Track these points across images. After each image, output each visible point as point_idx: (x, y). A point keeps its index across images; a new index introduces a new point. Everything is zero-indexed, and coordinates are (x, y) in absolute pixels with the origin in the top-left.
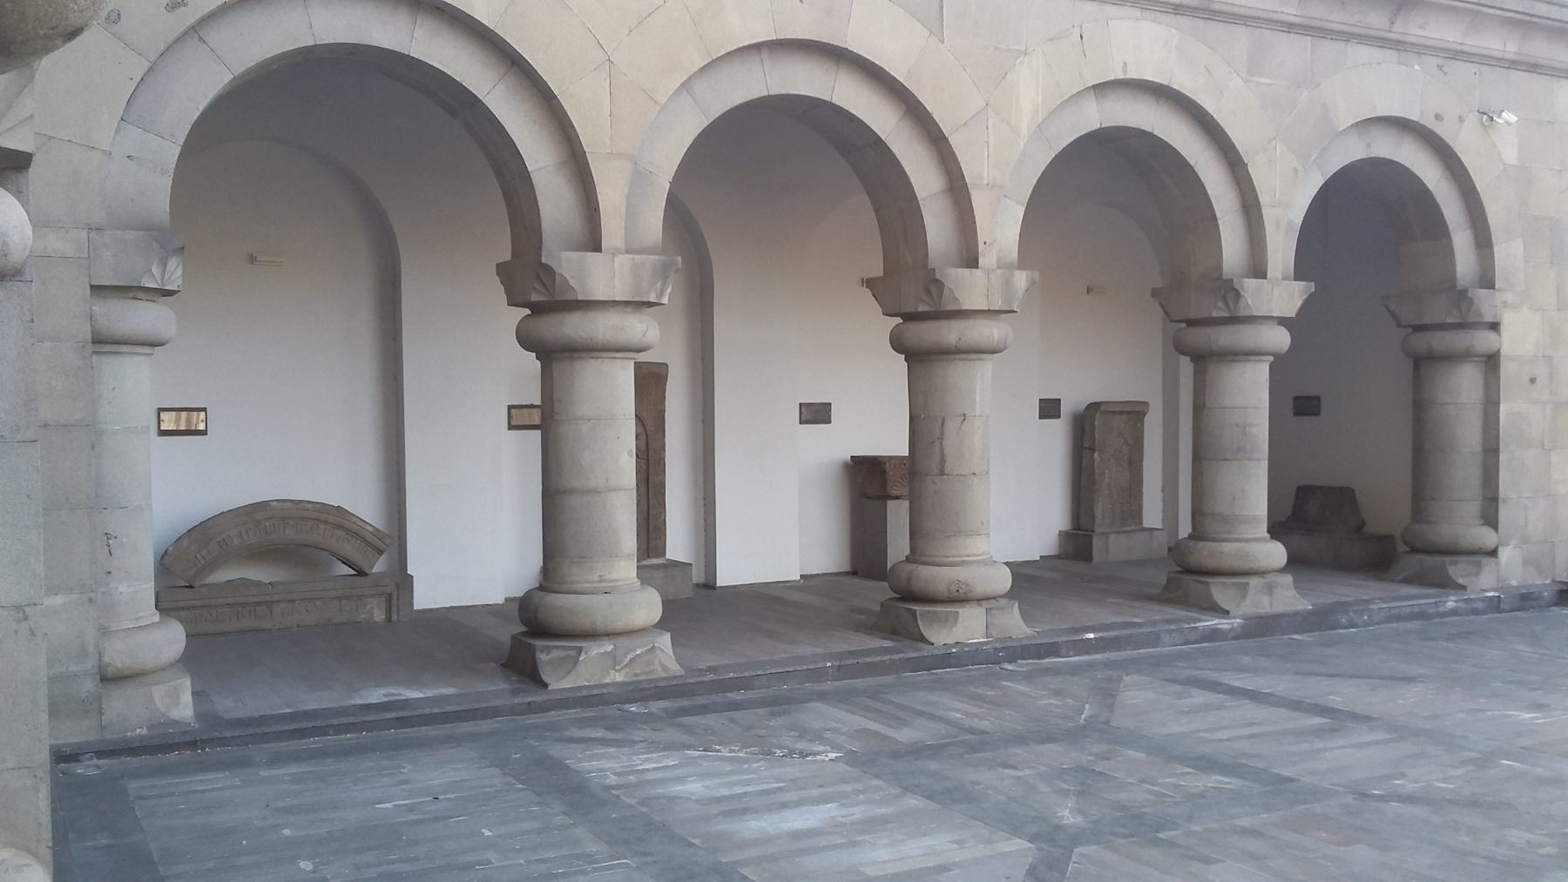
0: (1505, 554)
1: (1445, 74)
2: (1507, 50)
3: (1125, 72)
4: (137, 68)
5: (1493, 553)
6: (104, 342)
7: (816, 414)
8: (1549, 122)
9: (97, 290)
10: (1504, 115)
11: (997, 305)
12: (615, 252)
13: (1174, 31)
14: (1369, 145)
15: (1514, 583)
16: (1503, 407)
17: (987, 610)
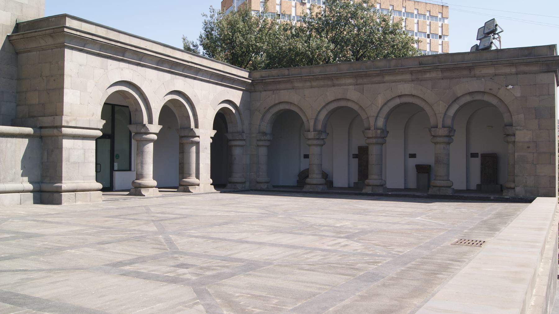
0: (517, 189)
3: (401, 93)
4: (261, 116)
5: (514, 188)
7: (413, 156)
10: (509, 86)
11: (374, 136)
12: (312, 132)
15: (521, 196)
16: (515, 154)
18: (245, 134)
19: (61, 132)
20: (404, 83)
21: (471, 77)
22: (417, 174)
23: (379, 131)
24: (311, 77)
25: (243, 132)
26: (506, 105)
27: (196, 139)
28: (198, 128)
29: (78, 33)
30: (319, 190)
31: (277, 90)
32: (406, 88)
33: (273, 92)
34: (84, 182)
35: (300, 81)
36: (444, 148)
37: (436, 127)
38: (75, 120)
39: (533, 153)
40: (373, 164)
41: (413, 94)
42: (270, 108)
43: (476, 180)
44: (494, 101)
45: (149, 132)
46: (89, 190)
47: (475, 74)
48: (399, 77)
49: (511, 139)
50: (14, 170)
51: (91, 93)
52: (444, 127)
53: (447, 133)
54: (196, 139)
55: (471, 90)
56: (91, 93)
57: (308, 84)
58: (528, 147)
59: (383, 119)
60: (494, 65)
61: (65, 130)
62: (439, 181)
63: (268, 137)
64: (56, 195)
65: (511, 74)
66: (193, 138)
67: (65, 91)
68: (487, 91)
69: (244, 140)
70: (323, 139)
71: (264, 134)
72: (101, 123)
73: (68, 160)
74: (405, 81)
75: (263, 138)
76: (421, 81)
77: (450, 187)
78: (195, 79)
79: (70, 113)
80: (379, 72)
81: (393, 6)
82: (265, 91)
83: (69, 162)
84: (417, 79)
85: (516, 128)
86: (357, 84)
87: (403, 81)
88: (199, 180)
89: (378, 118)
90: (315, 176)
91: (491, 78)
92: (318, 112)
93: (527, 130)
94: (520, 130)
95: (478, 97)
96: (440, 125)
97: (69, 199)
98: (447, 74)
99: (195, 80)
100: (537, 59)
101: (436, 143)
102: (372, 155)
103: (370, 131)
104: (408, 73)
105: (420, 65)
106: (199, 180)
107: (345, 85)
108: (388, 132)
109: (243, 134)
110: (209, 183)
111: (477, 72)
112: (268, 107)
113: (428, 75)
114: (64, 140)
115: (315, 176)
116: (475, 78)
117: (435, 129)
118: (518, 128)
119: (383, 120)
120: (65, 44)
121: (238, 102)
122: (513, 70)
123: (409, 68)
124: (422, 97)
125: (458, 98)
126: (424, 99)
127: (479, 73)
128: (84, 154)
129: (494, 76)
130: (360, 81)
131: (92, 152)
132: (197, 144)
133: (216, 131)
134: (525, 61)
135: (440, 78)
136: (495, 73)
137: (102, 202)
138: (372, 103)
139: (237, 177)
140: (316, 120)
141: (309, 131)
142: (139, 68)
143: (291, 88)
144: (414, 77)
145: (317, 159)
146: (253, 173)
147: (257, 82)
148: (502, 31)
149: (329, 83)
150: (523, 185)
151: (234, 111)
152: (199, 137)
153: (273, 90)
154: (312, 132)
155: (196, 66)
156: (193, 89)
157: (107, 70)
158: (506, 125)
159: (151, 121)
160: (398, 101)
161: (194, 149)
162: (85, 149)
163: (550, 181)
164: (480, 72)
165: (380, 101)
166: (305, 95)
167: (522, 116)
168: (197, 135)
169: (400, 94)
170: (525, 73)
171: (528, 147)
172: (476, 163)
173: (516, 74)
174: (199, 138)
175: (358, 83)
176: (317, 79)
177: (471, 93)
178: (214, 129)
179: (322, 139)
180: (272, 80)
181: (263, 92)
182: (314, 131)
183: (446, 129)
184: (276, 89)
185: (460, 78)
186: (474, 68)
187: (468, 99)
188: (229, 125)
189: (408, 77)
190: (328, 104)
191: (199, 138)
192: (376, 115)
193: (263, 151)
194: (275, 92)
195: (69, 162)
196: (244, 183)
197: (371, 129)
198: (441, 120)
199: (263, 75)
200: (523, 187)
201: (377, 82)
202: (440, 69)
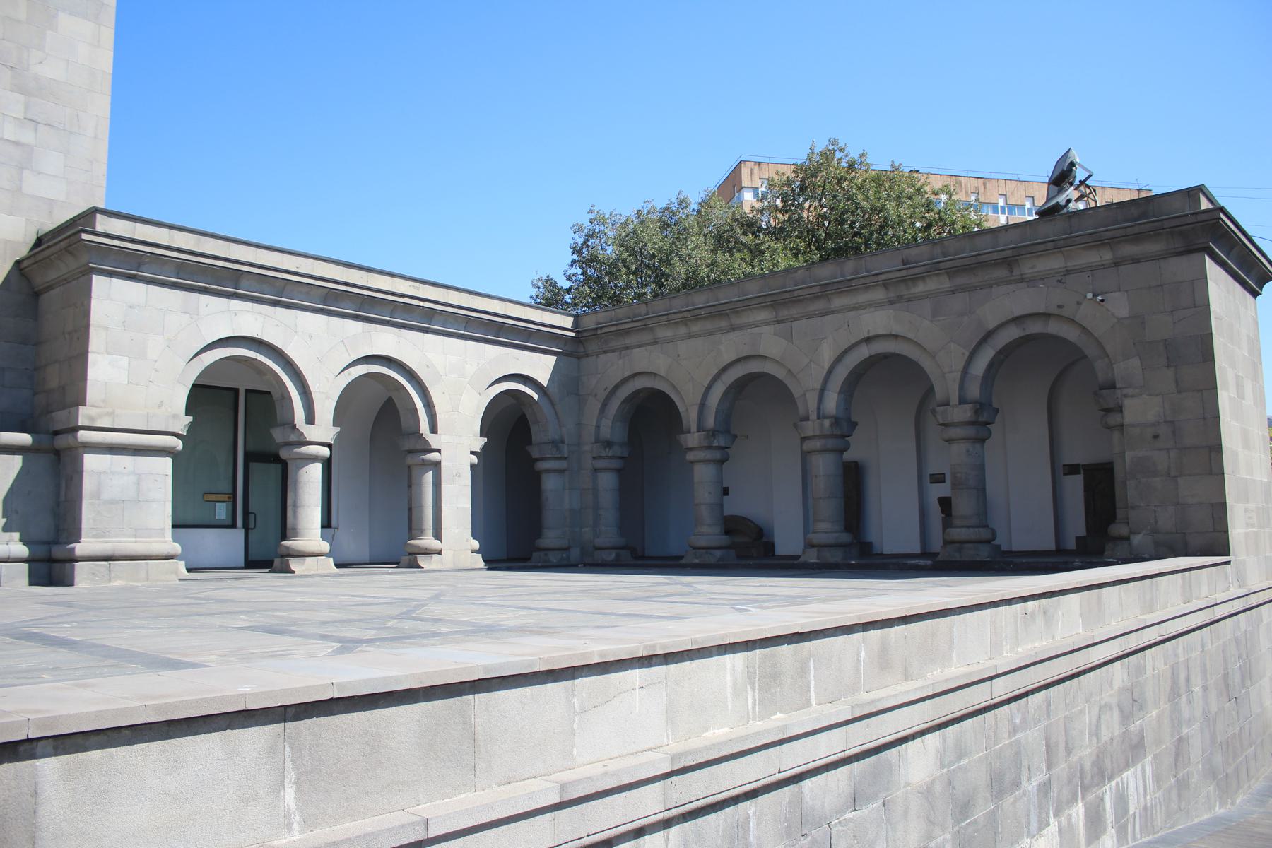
1: (1063, 283)
2: (1103, 259)
4: (599, 405)
5: (1128, 538)
6: (596, 470)
7: (938, 479)
8: (1158, 286)
9: (594, 458)
11: (818, 433)
12: (694, 433)
13: (891, 311)
14: (1024, 329)
17: (818, 551)
18: (566, 447)
19: (76, 438)
20: (873, 309)
21: (1016, 282)
22: (943, 517)
23: (827, 423)
24: (686, 314)
25: (563, 442)
26: (1097, 340)
27: (433, 456)
28: (437, 433)
29: (117, 243)
30: (713, 560)
31: (627, 348)
32: (877, 321)
33: (620, 354)
34: (136, 542)
35: (665, 324)
36: (968, 451)
37: (946, 404)
38: (111, 414)
39: (1168, 449)
40: (820, 498)
41: (893, 333)
42: (617, 387)
43: (1077, 525)
44: (1071, 334)
46: (146, 556)
47: (1022, 275)
48: (862, 298)
49: (1114, 419)
51: (156, 361)
52: (962, 401)
53: (969, 414)
54: (433, 456)
55: (1018, 313)
56: (156, 361)
57: (682, 330)
58: (1156, 437)
59: (836, 395)
60: (1059, 250)
61: (83, 436)
62: (958, 530)
63: (617, 451)
64: (68, 565)
65: (1103, 267)
67: (91, 357)
68: (1056, 311)
69: (565, 458)
70: (723, 448)
71: (608, 444)
72: (182, 423)
73: (97, 495)
74: (875, 305)
75: (603, 453)
76: (909, 300)
77: (988, 542)
78: (426, 331)
79: (104, 401)
80: (817, 289)
81: (1033, 197)
82: (605, 352)
84: (900, 298)
85: (1125, 391)
86: (778, 322)
87: (870, 305)
88: (441, 541)
89: (826, 393)
90: (704, 529)
91: (1059, 281)
92: (704, 388)
93: (1151, 395)
94: (1133, 396)
95: (1035, 328)
96: (954, 399)
97: (93, 574)
98: (961, 280)
99: (426, 334)
100: (1156, 224)
101: (950, 441)
102: (816, 476)
103: (810, 422)
104: (876, 285)
105: (904, 265)
106: (441, 541)
107: (755, 325)
108: (855, 425)
109: (561, 445)
110: (469, 547)
111: (1030, 267)
112: (610, 387)
113: (921, 288)
114: (86, 456)
115: (704, 529)
116: (1024, 284)
117: (945, 407)
118: (1130, 391)
119: (835, 395)
120: (90, 265)
121: (544, 378)
122: (1107, 256)
123: (877, 274)
124: (910, 335)
125: (988, 335)
126: (916, 342)
127: (1031, 271)
128: (138, 484)
129: (1065, 275)
130: (784, 313)
131: (157, 481)
132: (437, 465)
133: (486, 439)
134: (1129, 231)
135: (948, 291)
136: (1066, 267)
137: (177, 582)
138: (811, 361)
139: (551, 537)
140: (702, 406)
141: (689, 432)
142: (280, 310)
143: (652, 341)
144: (892, 294)
145: (710, 493)
146: (587, 529)
147: (585, 334)
148: (1090, 176)
149: (723, 323)
150: (1149, 527)
152: (439, 451)
153: (620, 350)
154: (694, 433)
155: (421, 304)
156: (422, 351)
157: (198, 315)
158: (1102, 388)
159: (310, 419)
160: (864, 352)
161: (429, 477)
162: (140, 475)
163: (1213, 515)
164: (1032, 268)
165: (827, 355)
166: (679, 356)
167: (1135, 362)
168: (434, 446)
169: (867, 335)
170: (1135, 260)
171: (1156, 437)
172: (1075, 487)
173: (1115, 266)
174: (440, 452)
175: (780, 319)
176: (698, 318)
177: (1018, 320)
178: (482, 435)
179: (716, 447)
180: (614, 328)
181: (602, 356)
182: (698, 431)
183: (968, 407)
184: (624, 346)
185: (992, 287)
186: (1017, 260)
187: (1013, 333)
188: (534, 429)
189: (879, 295)
190: (725, 369)
191: (440, 452)
192: (818, 386)
193: (607, 481)
194: (623, 352)
196: (566, 549)
197: (810, 418)
198: (957, 386)
199: (601, 321)
200: (1147, 534)
201: (817, 312)
202: (943, 271)
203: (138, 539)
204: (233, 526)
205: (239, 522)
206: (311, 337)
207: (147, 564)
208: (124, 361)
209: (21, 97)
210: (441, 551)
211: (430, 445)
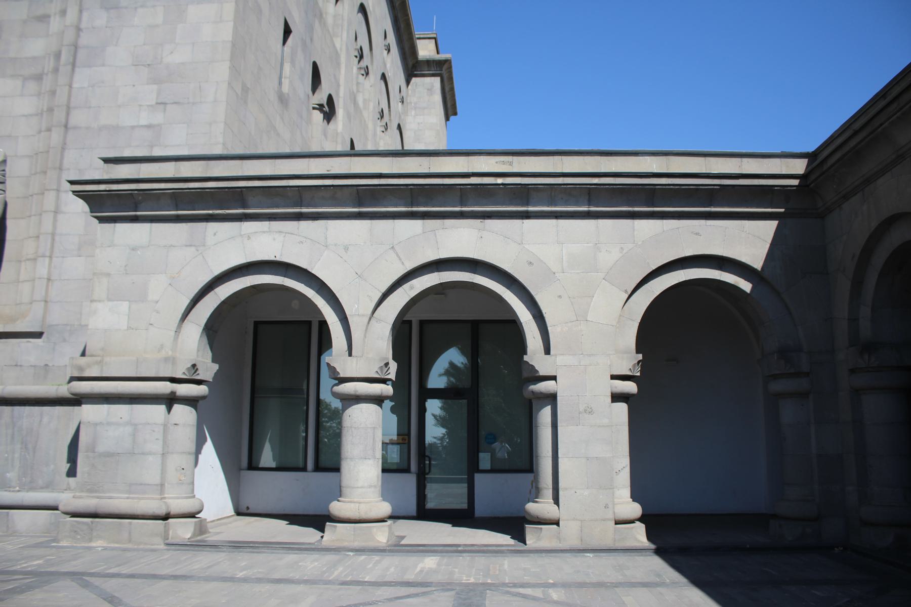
29: (102, 187)
38: (100, 363)
45: (537, 375)
46: (124, 515)
50: (52, 467)
51: (157, 302)
56: (157, 302)
66: (535, 384)
73: (92, 448)
78: (527, 216)
79: (102, 349)
83: (94, 452)
97: (76, 531)
99: (525, 221)
110: (610, 515)
121: (755, 256)
128: (134, 435)
131: (154, 431)
132: (551, 398)
137: (162, 547)
142: (304, 224)
151: (746, 286)
152: (554, 378)
155: (500, 181)
162: (136, 425)
168: (542, 372)
195: (94, 452)
203: (131, 496)
204: (407, 470)
205: (414, 467)
206: (346, 249)
207: (130, 523)
208: (124, 306)
209: (155, 87)
210: (559, 520)
211: (537, 371)
